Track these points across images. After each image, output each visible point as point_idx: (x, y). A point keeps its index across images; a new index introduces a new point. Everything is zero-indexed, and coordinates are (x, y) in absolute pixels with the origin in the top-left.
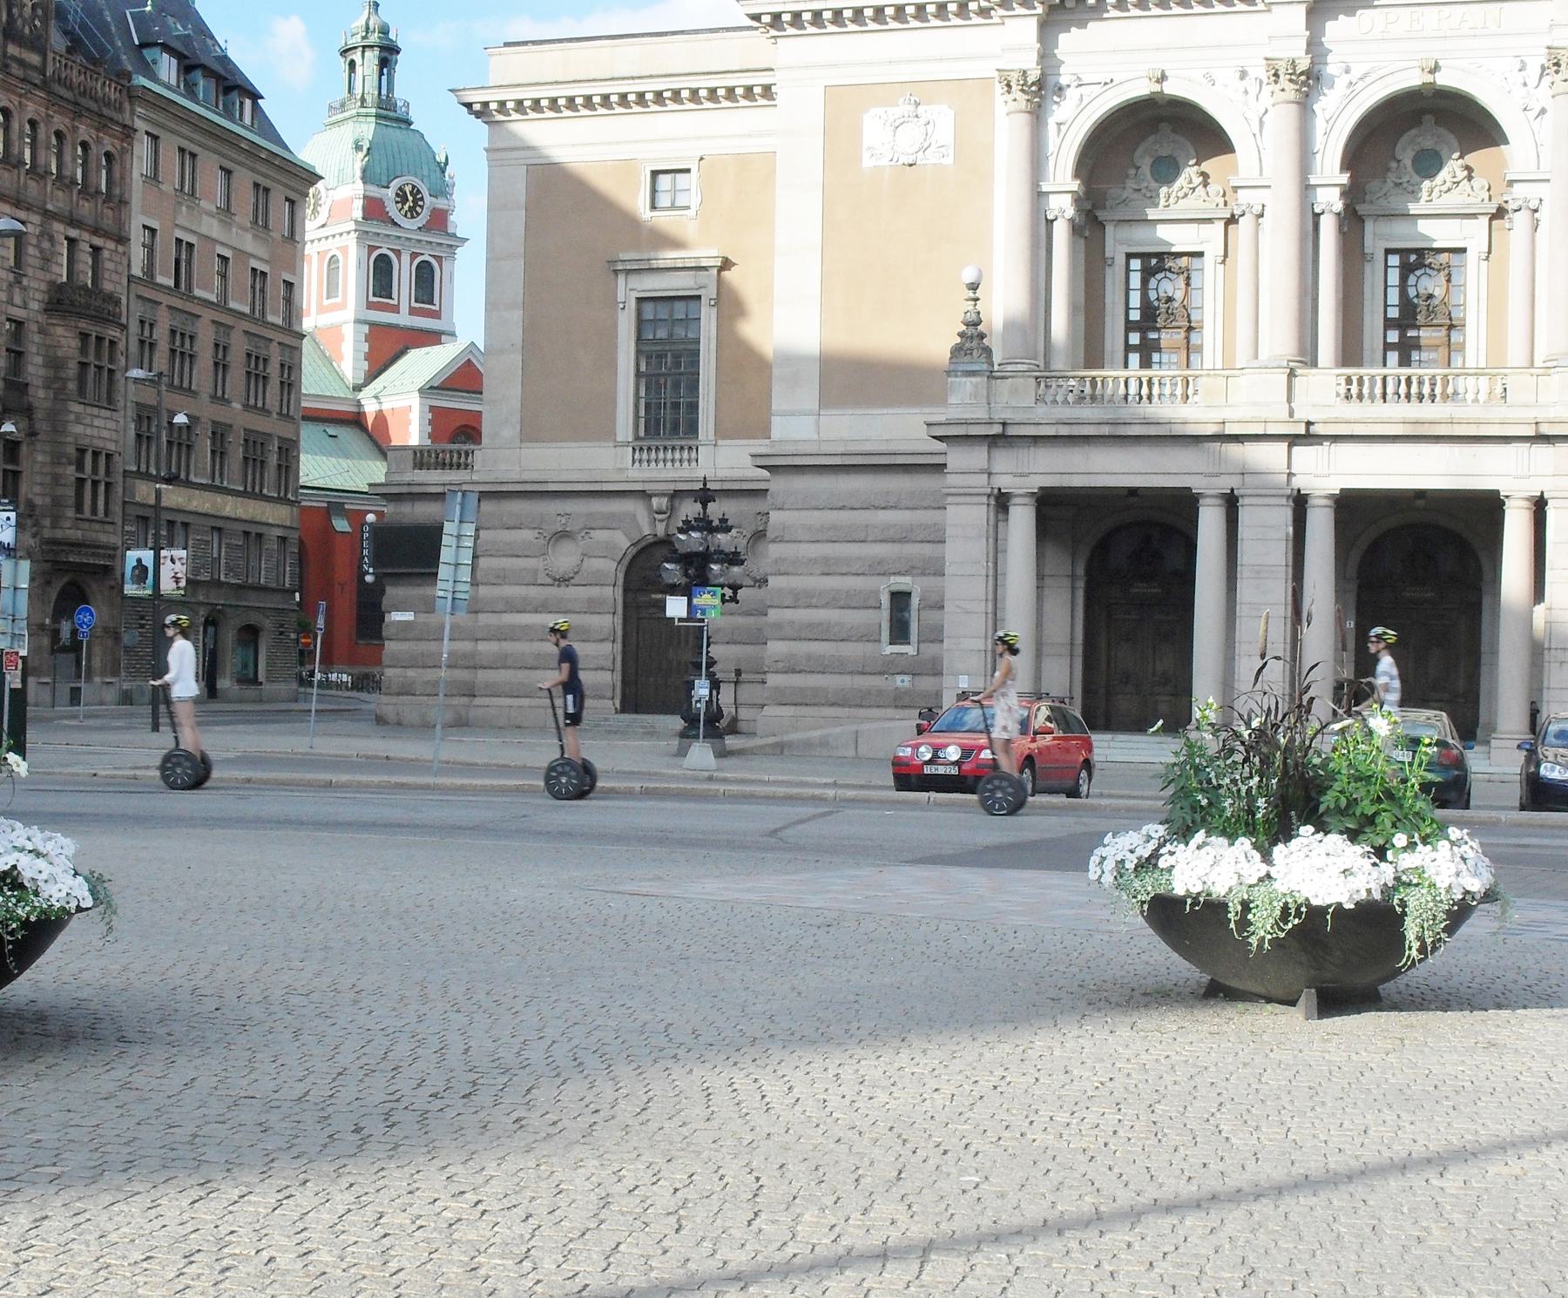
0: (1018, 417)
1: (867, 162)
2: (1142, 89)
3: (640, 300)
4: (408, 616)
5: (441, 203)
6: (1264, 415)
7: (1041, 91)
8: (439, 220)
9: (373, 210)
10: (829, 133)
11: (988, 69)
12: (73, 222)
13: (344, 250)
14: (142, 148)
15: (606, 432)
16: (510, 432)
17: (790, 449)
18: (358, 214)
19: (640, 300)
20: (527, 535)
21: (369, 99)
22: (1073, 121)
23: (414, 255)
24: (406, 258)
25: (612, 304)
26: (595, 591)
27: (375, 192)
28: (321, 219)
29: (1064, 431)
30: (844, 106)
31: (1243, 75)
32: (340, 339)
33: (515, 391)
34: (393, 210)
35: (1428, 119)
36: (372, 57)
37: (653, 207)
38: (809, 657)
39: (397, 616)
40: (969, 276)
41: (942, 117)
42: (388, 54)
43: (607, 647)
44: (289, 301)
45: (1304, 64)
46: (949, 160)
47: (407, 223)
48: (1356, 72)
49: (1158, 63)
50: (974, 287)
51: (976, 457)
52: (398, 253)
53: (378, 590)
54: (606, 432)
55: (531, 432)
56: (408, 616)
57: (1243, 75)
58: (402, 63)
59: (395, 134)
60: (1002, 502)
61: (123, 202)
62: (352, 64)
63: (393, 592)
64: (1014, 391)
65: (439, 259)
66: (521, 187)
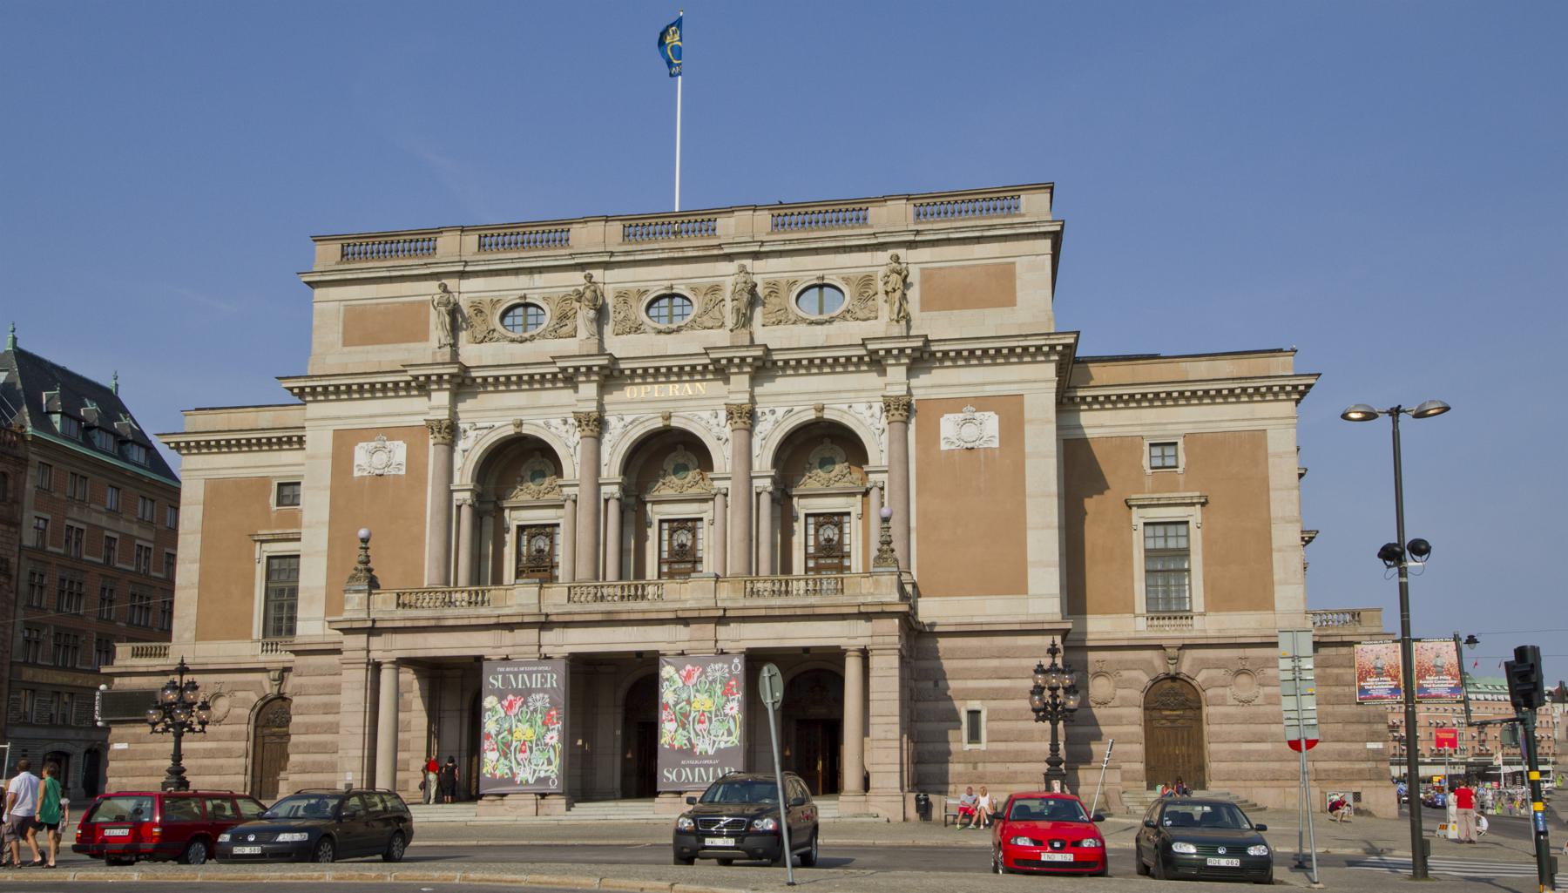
0: (386, 616)
1: (357, 473)
2: (511, 431)
3: (269, 558)
4: (124, 746)
6: (525, 611)
7: (450, 432)
11: (419, 421)
16: (189, 635)
17: (307, 640)
19: (269, 558)
25: (252, 560)
26: (236, 728)
29: (409, 624)
31: (565, 422)
33: (193, 610)
35: (680, 447)
37: (279, 504)
38: (314, 763)
39: (117, 746)
40: (363, 533)
41: (399, 450)
43: (242, 760)
45: (595, 415)
46: (403, 472)
48: (628, 419)
49: (519, 415)
50: (365, 540)
53: (107, 730)
56: (124, 746)
57: (565, 422)
63: (116, 731)
64: (384, 602)
66: (201, 492)
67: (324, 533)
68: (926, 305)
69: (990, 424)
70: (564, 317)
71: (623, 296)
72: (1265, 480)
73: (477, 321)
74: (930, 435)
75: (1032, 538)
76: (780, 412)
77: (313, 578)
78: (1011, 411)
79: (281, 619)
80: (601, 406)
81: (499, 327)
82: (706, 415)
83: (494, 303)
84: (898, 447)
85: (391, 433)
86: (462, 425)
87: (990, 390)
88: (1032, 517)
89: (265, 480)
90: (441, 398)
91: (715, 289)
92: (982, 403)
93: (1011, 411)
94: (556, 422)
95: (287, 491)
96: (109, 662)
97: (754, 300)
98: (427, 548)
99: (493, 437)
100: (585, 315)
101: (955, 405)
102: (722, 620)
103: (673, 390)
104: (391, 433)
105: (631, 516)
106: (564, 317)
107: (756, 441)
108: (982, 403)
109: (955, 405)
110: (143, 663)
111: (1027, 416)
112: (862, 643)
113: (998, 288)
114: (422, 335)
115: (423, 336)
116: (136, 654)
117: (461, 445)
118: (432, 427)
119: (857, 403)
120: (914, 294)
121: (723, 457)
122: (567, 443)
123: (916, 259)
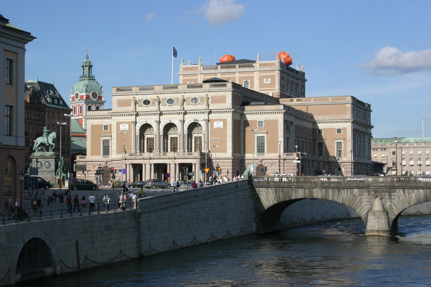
2: (145, 123)
5: (101, 95)
8: (100, 98)
9: (88, 97)
10: (117, 127)
12: (39, 125)
13: (83, 105)
14: (47, 113)
15: (100, 155)
16: (90, 154)
18: (85, 98)
20: (91, 166)
21: (87, 76)
22: (139, 126)
23: (96, 105)
24: (94, 106)
27: (88, 94)
28: (79, 99)
30: (118, 124)
32: (82, 121)
33: (90, 150)
34: (91, 97)
36: (88, 68)
41: (127, 126)
42: (90, 67)
44: (68, 128)
47: (94, 100)
51: (124, 161)
52: (92, 105)
53: (76, 172)
54: (100, 155)
55: (92, 154)
58: (94, 69)
59: (92, 82)
60: (126, 165)
61: (45, 121)
62: (84, 69)
65: (101, 105)
67: (116, 140)
68: (212, 102)
69: (222, 123)
70: (153, 103)
71: (163, 99)
72: (278, 129)
73: (139, 103)
74: (212, 125)
75: (228, 143)
76: (188, 120)
77: (113, 146)
78: (225, 121)
79: (106, 152)
80: (160, 119)
81: (143, 104)
82: (177, 121)
83: (142, 100)
84: (207, 128)
85: (126, 123)
86: (137, 122)
87: (222, 118)
88: (228, 140)
89: (102, 125)
90: (134, 117)
91: (178, 98)
92: (220, 120)
93: (225, 121)
94: (152, 121)
95: (106, 127)
96: (75, 159)
97: (184, 100)
98: (132, 145)
99: (142, 124)
100: (157, 103)
101: (216, 120)
102: (175, 159)
103: (171, 116)
104: (126, 123)
105: (166, 136)
106: (153, 103)
107: (185, 125)
108: (220, 120)
109: (216, 120)
110: (82, 160)
111: (227, 122)
112: (195, 162)
113: (223, 100)
114: (130, 105)
115: (130, 105)
116: (80, 158)
117: (137, 125)
118: (132, 122)
119: (201, 118)
120: (210, 100)
121: (179, 127)
122: (154, 125)
123: (210, 95)
